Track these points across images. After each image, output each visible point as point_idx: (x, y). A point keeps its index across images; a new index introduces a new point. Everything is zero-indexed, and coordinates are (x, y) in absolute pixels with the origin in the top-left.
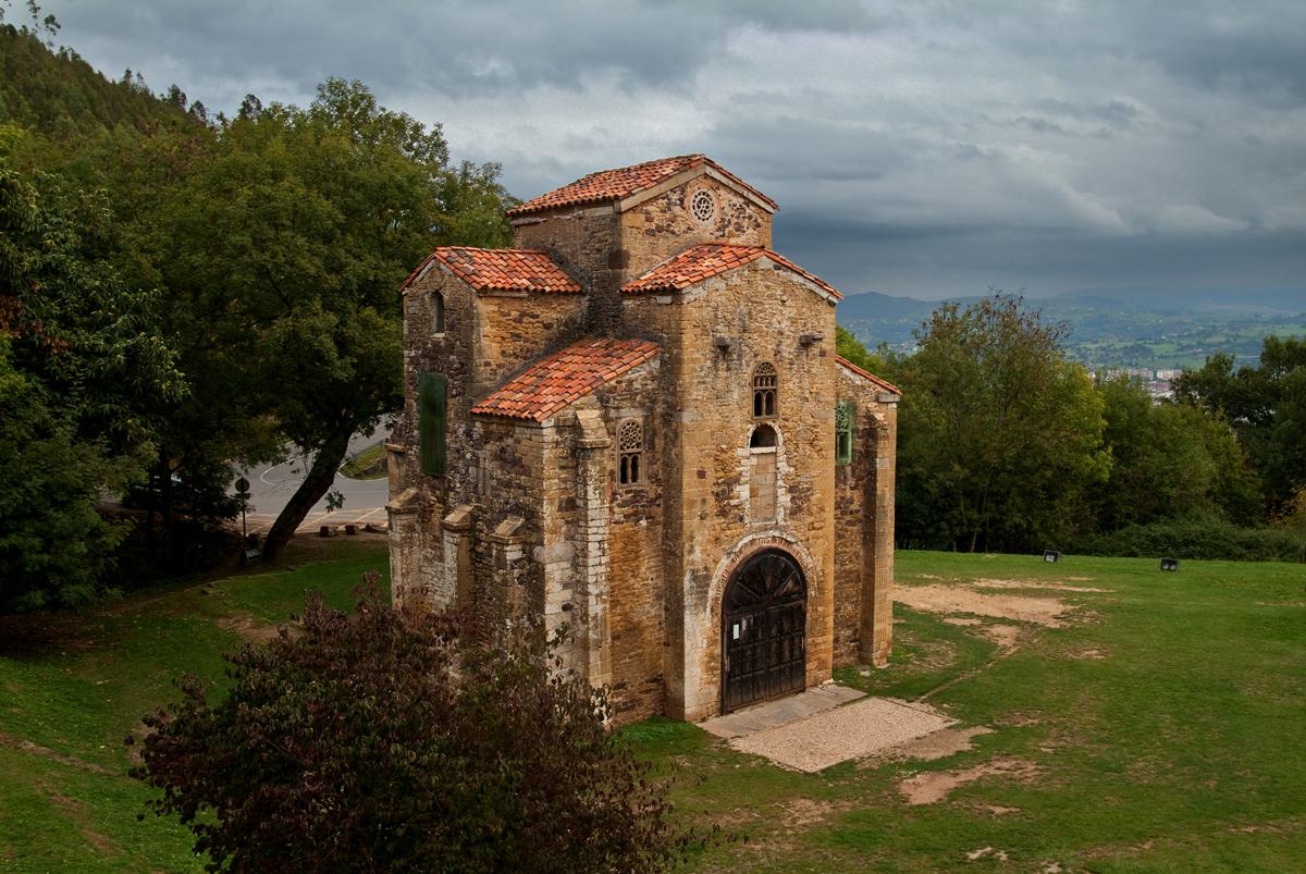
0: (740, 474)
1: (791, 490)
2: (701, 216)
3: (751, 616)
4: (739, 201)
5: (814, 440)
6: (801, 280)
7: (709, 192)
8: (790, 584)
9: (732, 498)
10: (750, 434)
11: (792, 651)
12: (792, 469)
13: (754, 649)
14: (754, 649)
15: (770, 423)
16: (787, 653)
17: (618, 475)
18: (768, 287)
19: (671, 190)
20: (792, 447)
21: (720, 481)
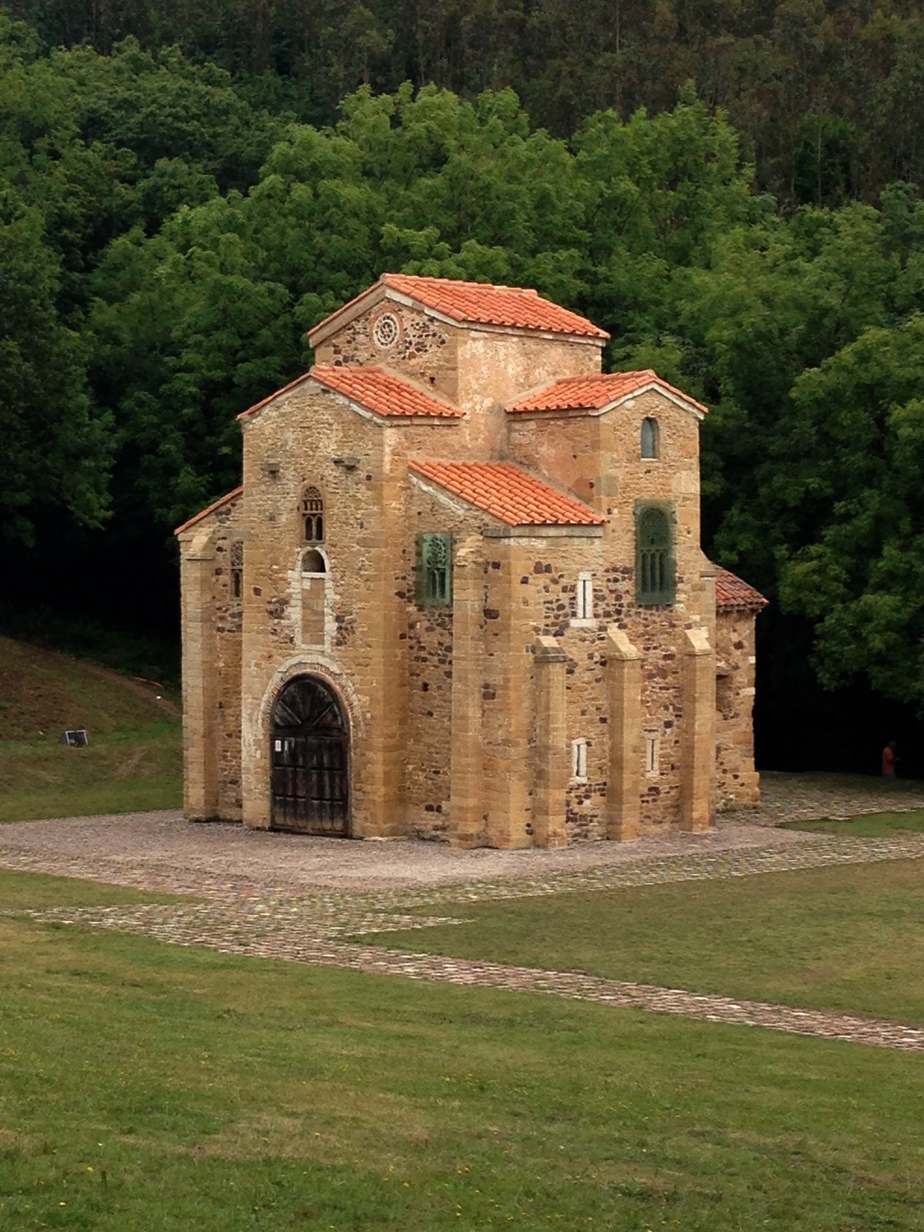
0: (290, 595)
1: (338, 619)
2: (383, 340)
3: (292, 739)
4: (418, 319)
5: (360, 569)
6: (347, 402)
7: (393, 316)
8: (330, 717)
9: (283, 618)
10: (300, 558)
11: (332, 788)
12: (338, 597)
13: (295, 774)
14: (295, 774)
15: (317, 548)
16: (327, 790)
17: (231, 587)
18: (316, 411)
19: (355, 319)
20: (338, 576)
21: (274, 600)
